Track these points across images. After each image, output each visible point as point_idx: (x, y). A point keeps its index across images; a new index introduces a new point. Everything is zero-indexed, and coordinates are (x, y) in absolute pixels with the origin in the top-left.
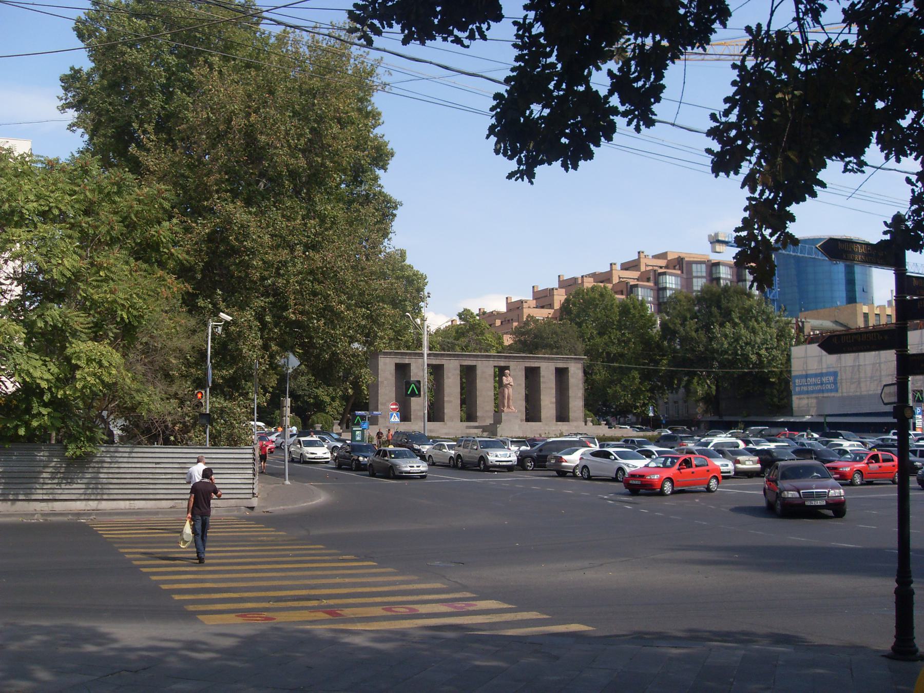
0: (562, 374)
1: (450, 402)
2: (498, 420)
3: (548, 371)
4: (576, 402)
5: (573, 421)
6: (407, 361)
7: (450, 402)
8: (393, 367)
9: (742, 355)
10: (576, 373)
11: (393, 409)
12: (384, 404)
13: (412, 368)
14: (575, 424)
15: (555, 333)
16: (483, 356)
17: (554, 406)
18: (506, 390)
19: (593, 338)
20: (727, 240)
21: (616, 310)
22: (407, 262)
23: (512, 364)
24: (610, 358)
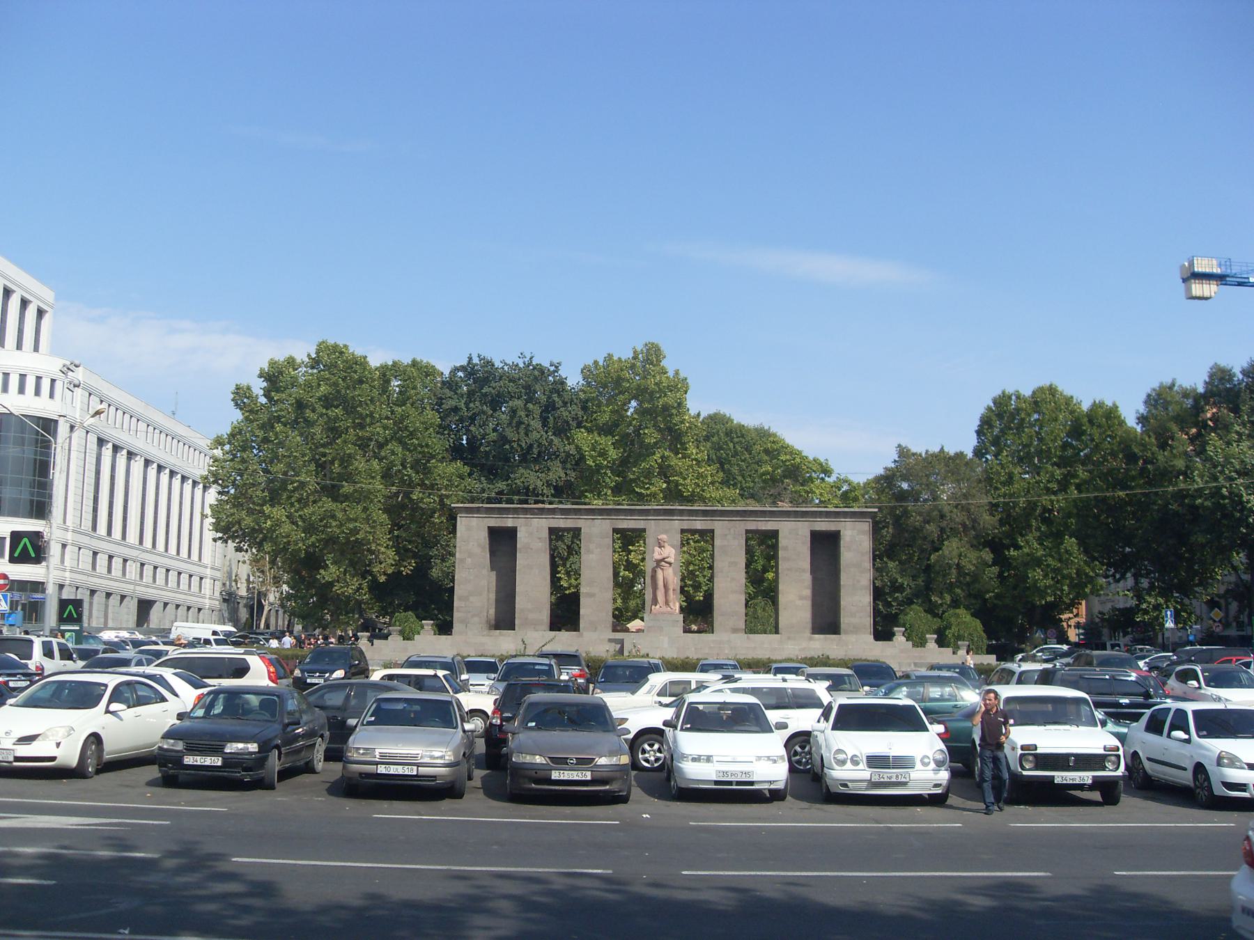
1: (591, 595)
3: (794, 542)
4: (857, 600)
5: (846, 633)
6: (509, 523)
7: (591, 595)
8: (485, 534)
16: (657, 512)
18: (660, 573)
20: (1217, 270)
23: (720, 527)
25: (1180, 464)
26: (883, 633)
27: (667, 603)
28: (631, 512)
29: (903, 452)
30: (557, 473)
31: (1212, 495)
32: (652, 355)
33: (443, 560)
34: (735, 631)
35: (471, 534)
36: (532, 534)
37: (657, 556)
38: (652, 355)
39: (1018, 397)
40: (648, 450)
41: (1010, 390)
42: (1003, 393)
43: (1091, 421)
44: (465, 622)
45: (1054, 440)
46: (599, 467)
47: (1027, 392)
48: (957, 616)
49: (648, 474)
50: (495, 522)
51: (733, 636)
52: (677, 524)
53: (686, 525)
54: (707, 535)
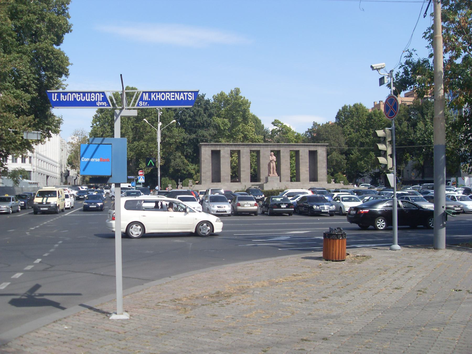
0: (313, 155)
1: (244, 171)
2: (267, 181)
4: (322, 170)
5: (320, 181)
6: (218, 149)
7: (244, 171)
8: (210, 152)
9: (428, 140)
10: (322, 153)
11: (141, 175)
12: (205, 173)
13: (222, 152)
14: (321, 183)
15: (328, 132)
16: (263, 145)
17: (308, 172)
19: (351, 134)
21: (365, 117)
22: (240, 95)
24: (362, 144)
25: (406, 129)
26: (329, 182)
27: (273, 173)
28: (256, 145)
29: (315, 124)
30: (212, 131)
31: (422, 140)
32: (237, 91)
33: (174, 160)
34: (287, 181)
35: (206, 152)
36: (225, 152)
37: (271, 159)
38: (237, 91)
39: (350, 107)
40: (239, 123)
41: (347, 105)
42: (345, 105)
43: (375, 115)
44: (205, 180)
45: (364, 121)
46: (225, 129)
47: (352, 105)
48: (339, 175)
49: (239, 131)
50: (214, 148)
51: (287, 183)
52: (269, 149)
53: (272, 149)
54: (297, 152)
